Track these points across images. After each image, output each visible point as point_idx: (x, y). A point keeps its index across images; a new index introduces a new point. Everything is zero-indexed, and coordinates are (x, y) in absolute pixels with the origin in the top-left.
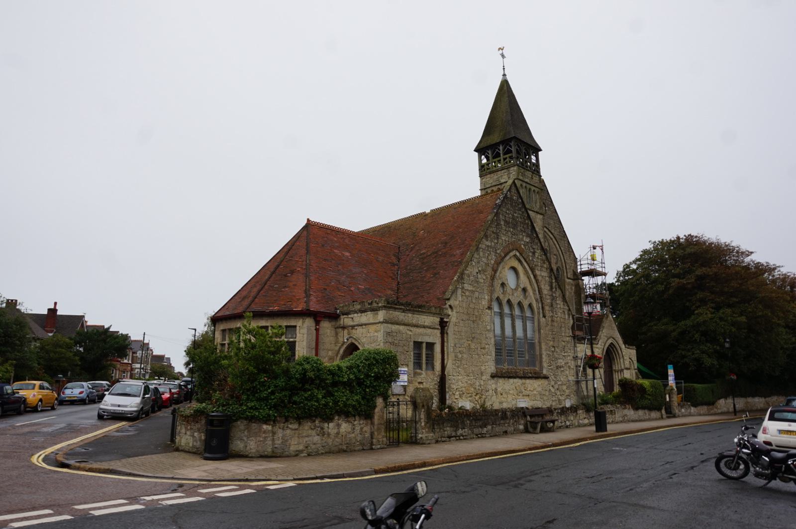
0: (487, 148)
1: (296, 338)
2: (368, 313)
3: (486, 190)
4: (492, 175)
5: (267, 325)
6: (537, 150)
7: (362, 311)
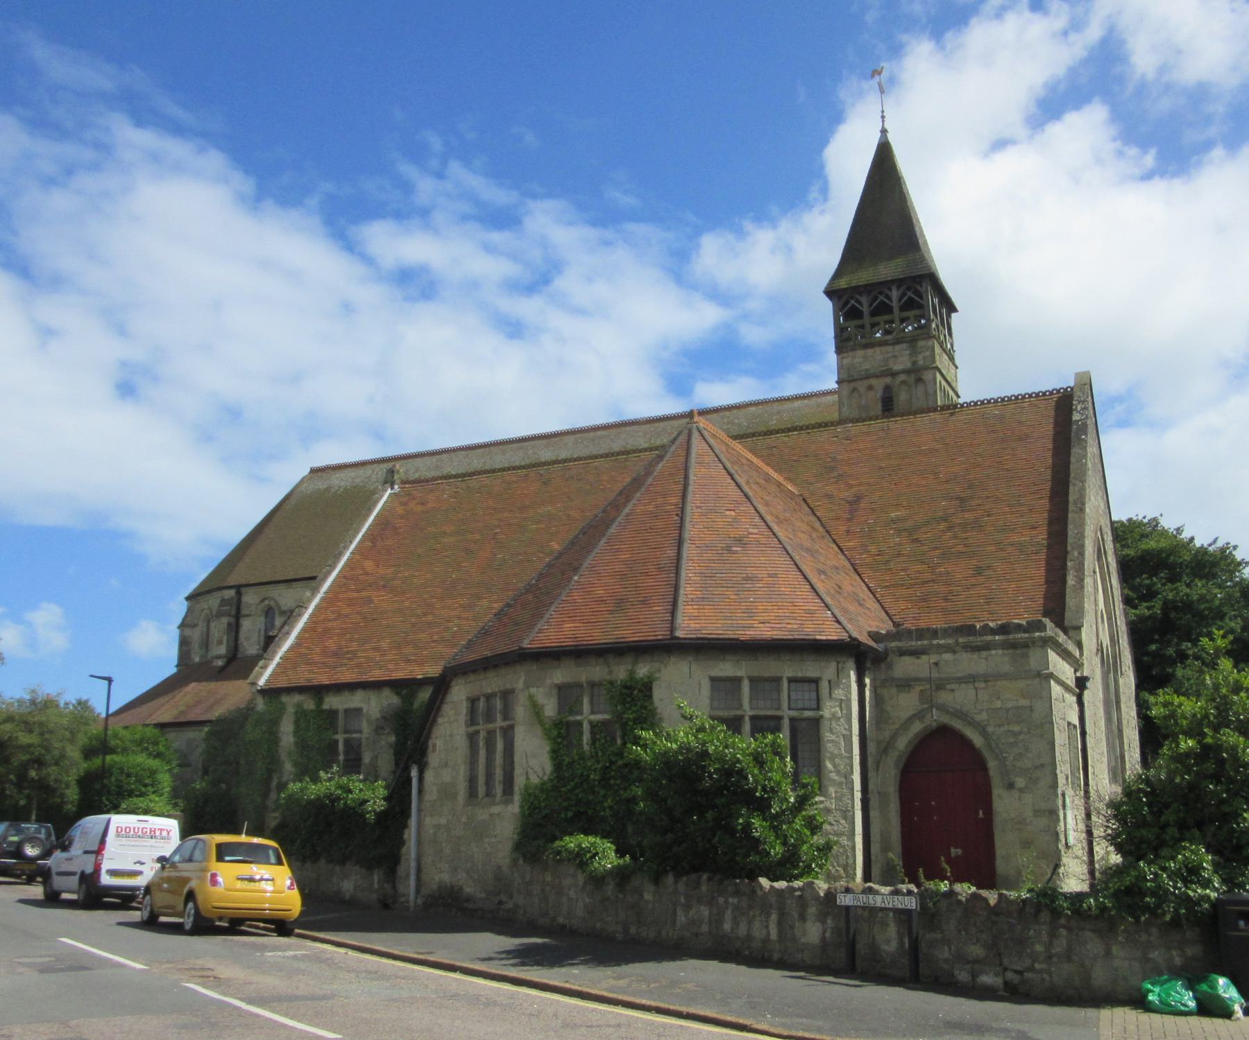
0: (857, 290)
1: (818, 708)
2: (993, 652)
3: (853, 385)
4: (870, 352)
5: (739, 674)
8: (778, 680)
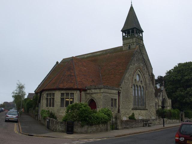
6: (142, 32)
7: (95, 89)
8: (69, 93)
